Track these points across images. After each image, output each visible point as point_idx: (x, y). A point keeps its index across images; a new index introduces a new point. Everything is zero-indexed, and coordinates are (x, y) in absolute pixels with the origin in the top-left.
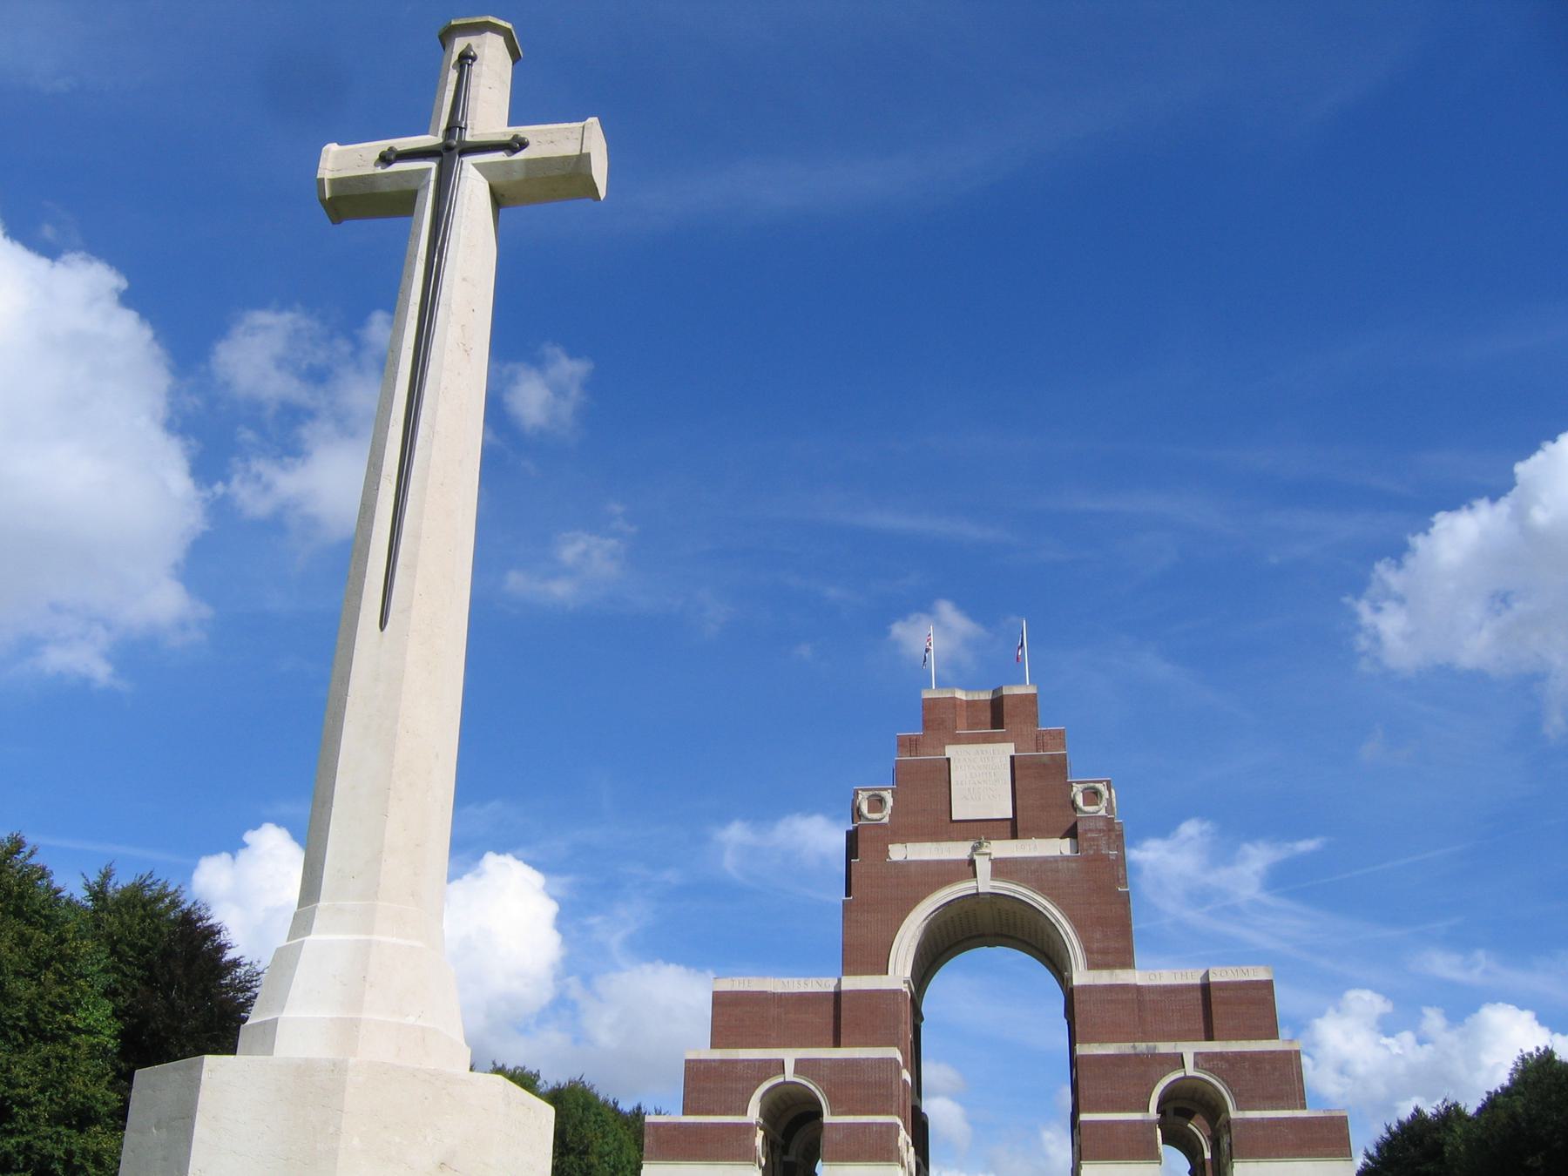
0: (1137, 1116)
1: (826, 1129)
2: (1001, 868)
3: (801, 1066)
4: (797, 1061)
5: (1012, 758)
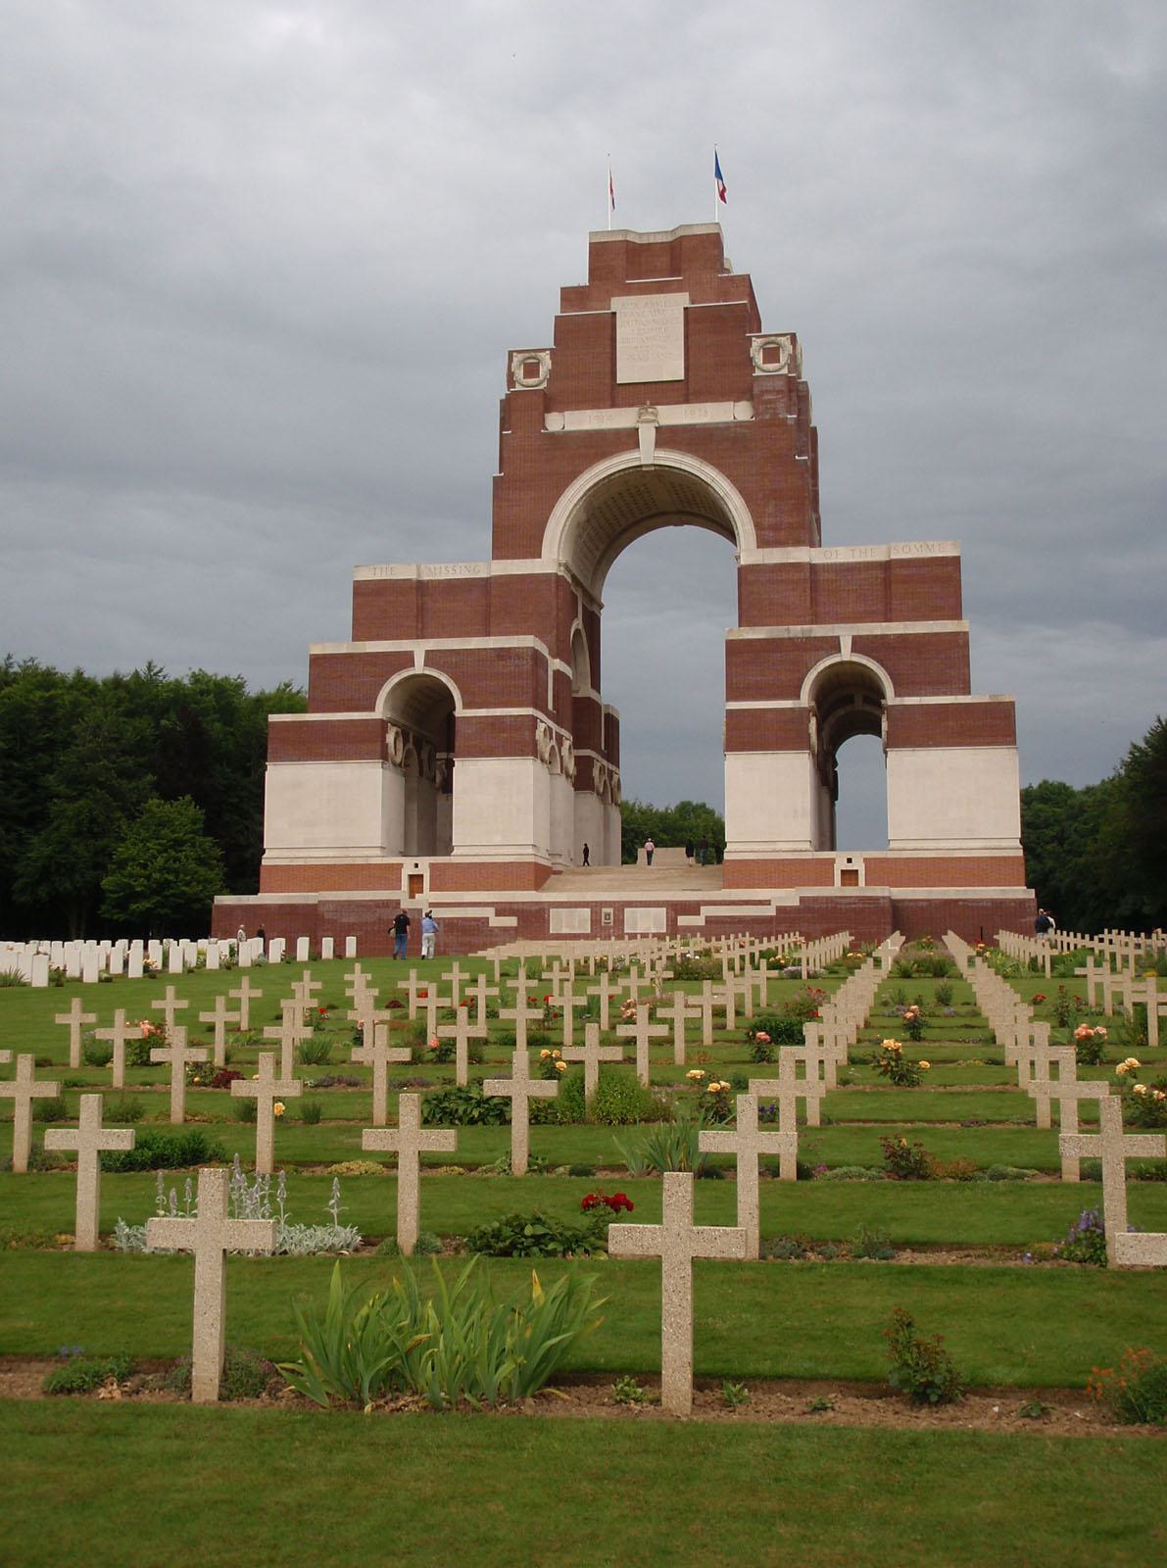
1: (458, 724)
2: (668, 437)
3: (432, 658)
4: (428, 652)
5: (685, 309)
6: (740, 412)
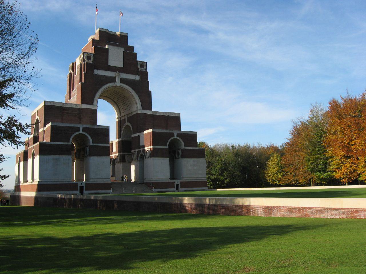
2: (122, 81)
6: (137, 78)
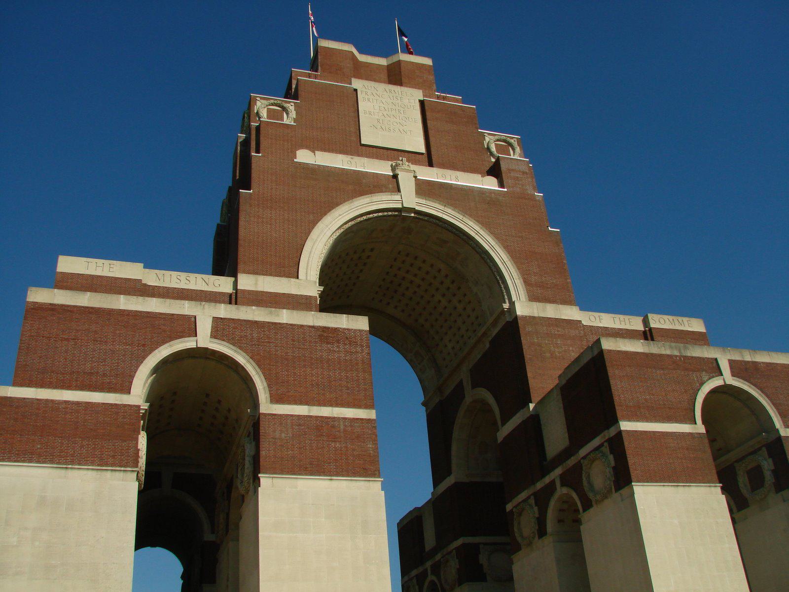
0: (684, 428)
2: (424, 189)
3: (220, 328)
4: (216, 320)
5: (420, 101)
